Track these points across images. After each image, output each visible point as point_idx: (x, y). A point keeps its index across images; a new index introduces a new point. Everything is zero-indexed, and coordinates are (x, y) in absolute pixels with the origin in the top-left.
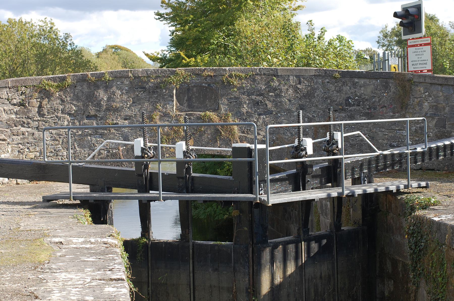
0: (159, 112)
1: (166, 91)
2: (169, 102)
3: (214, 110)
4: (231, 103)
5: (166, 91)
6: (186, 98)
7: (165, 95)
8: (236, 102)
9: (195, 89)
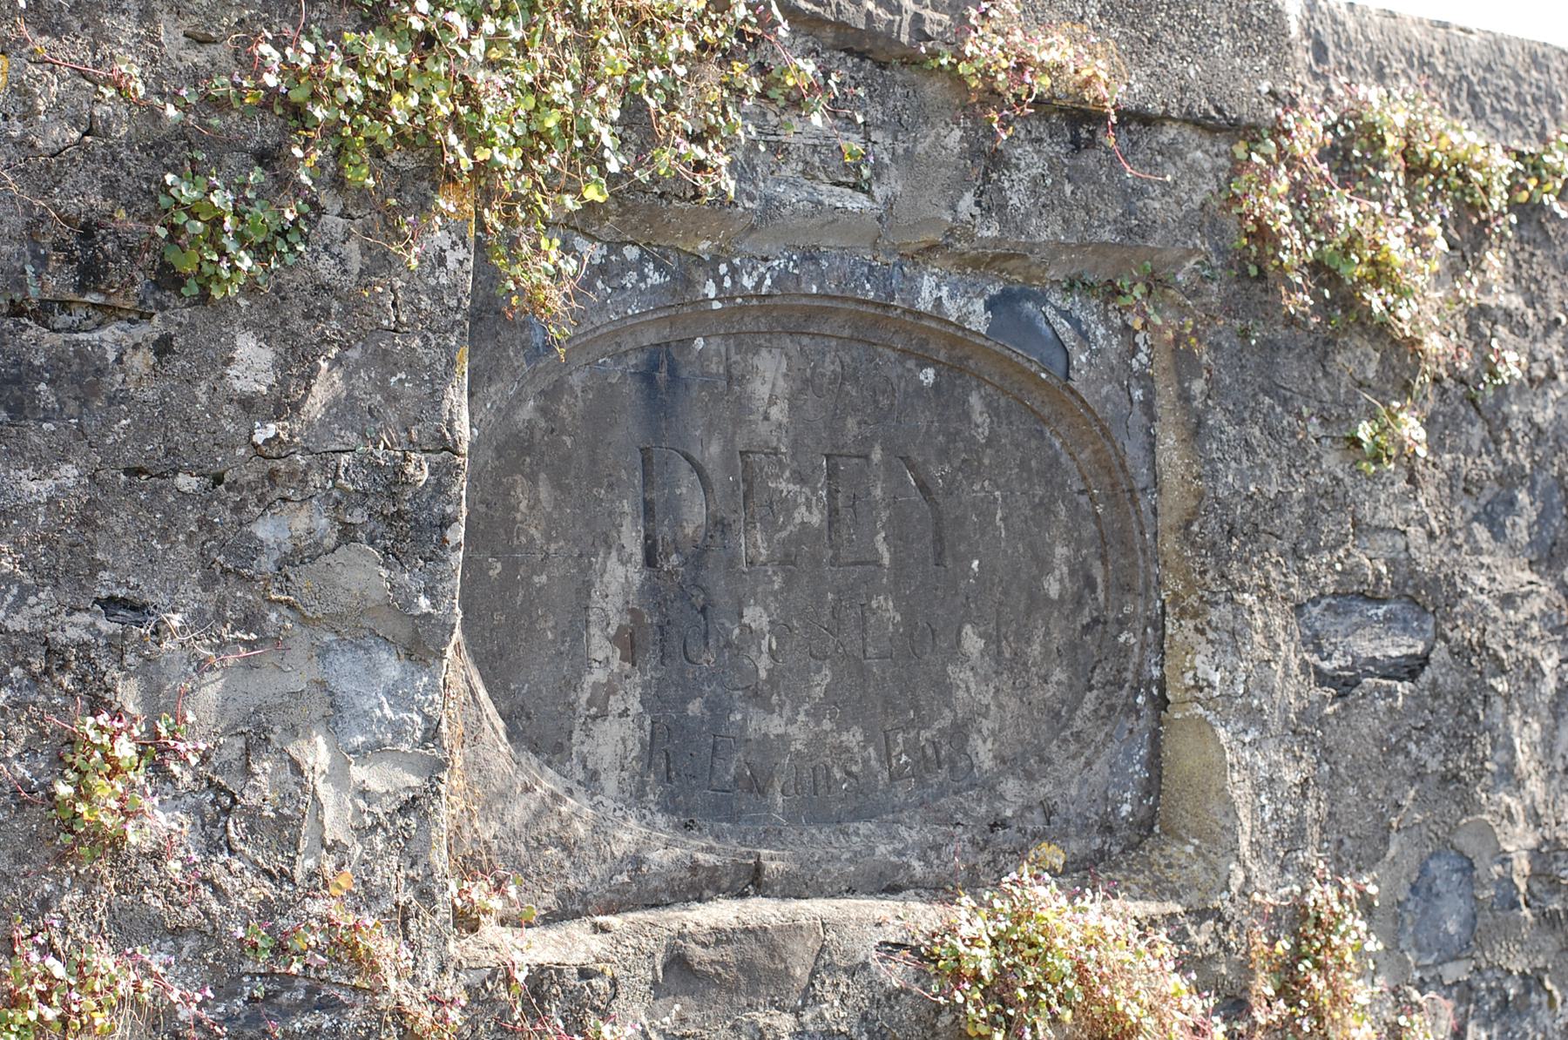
0: (129, 929)
1: (297, 362)
2: (344, 671)
3: (1113, 850)
4: (1344, 685)
5: (297, 362)
6: (619, 578)
7: (275, 480)
8: (1411, 668)
9: (769, 376)
